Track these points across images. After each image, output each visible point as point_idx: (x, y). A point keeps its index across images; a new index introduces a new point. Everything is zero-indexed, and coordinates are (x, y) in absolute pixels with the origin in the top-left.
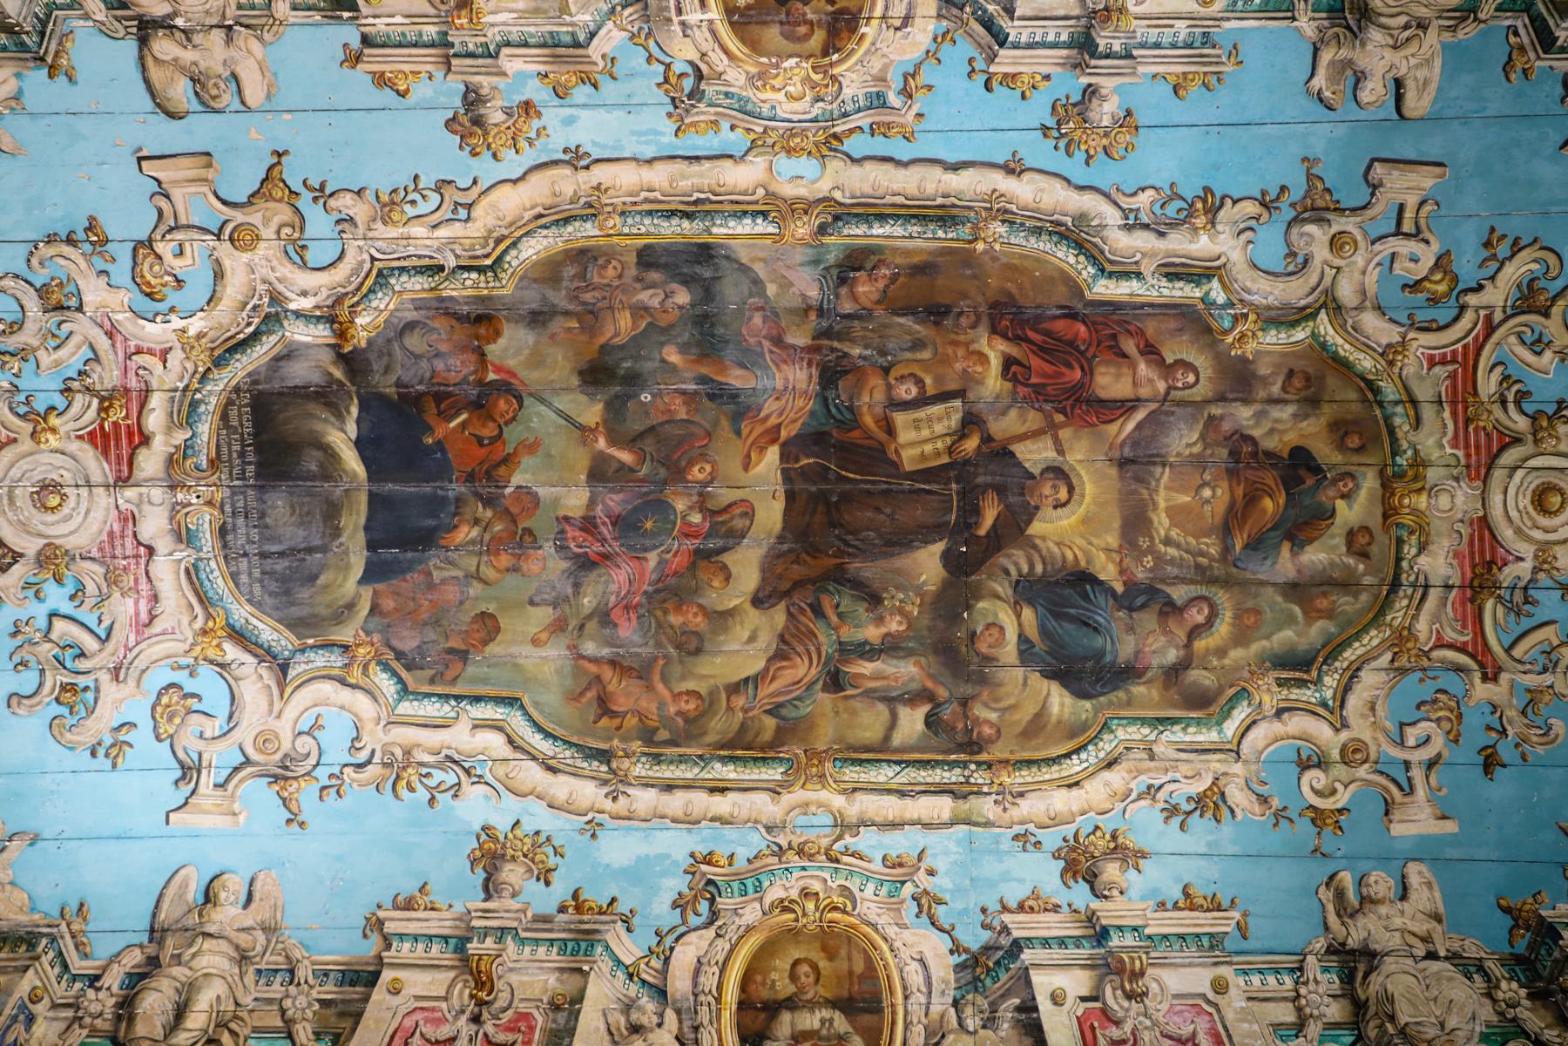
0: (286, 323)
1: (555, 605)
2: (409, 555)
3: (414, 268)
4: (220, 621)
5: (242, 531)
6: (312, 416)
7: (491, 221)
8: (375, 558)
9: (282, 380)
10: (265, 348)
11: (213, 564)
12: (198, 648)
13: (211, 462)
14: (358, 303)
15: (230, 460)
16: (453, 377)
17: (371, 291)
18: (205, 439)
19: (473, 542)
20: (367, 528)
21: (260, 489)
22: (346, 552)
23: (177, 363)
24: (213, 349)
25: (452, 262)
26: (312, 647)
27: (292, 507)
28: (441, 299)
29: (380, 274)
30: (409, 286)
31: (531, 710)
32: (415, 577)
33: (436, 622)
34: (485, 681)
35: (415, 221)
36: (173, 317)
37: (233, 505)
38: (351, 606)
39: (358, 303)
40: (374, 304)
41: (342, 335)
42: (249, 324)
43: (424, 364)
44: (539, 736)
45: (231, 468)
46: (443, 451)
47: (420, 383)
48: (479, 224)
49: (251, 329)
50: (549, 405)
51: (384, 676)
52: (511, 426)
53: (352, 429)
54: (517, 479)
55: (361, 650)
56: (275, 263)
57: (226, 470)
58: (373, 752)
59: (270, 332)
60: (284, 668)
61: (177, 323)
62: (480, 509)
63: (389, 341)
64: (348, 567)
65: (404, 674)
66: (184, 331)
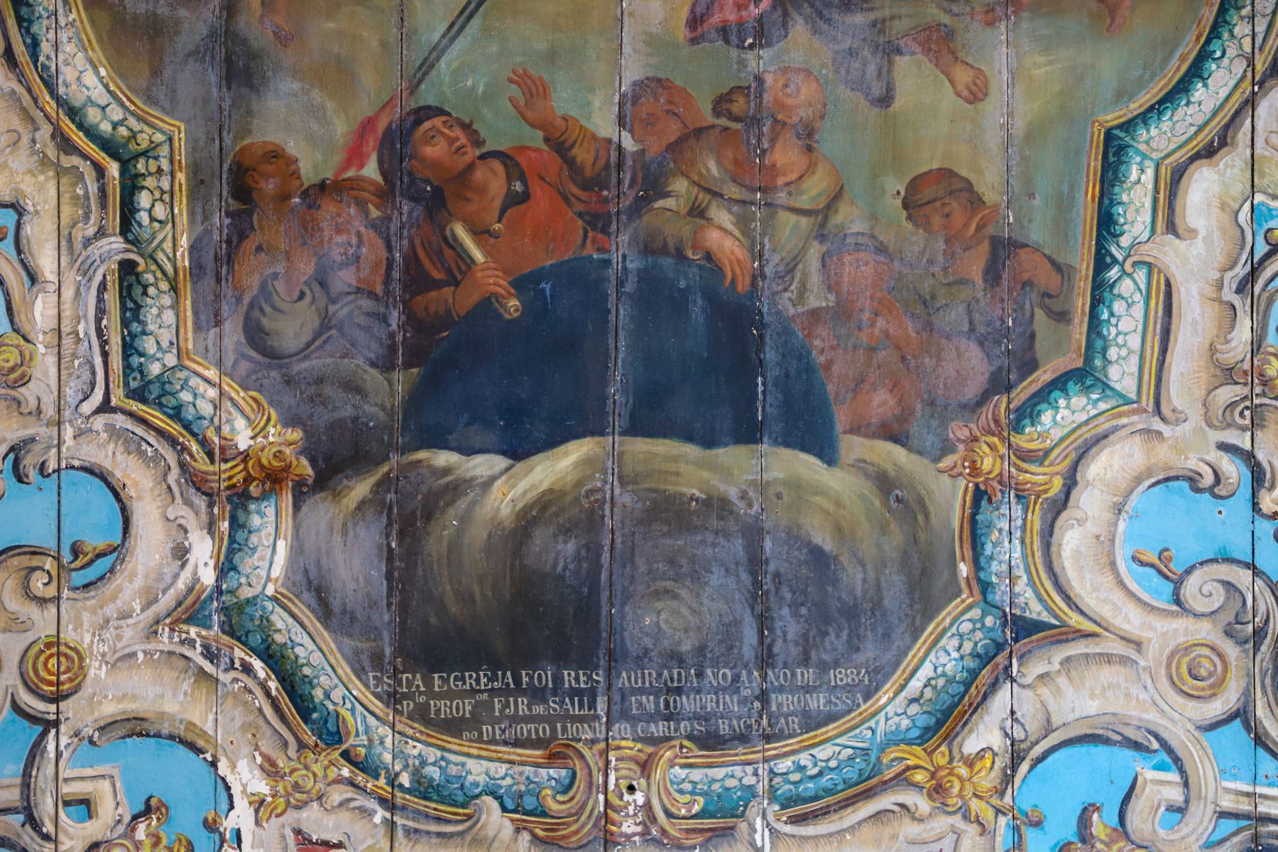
0: (246, 593)
1: (892, 50)
2: (770, 355)
3: (125, 323)
4: (915, 755)
5: (709, 702)
6: (454, 547)
7: (21, 161)
8: (778, 428)
9: (373, 604)
10: (301, 637)
11: (784, 765)
12: (975, 805)
13: (554, 758)
14: (204, 443)
15: (549, 720)
16: (373, 249)
17: (176, 414)
18: (503, 769)
19: (744, 222)
20: (709, 441)
21: (615, 659)
22: (762, 487)
23: (330, 821)
24: (302, 745)
25: (114, 245)
26: (977, 566)
27: (657, 595)
28: (197, 269)
29: (139, 395)
30: (166, 336)
31: (1135, 107)
32: (821, 345)
33: (927, 304)
34: (1064, 205)
35: (21, 319)
36: (229, 824)
37: (651, 718)
38: (885, 483)
39: (204, 443)
40: (206, 409)
41: (274, 479)
42: (247, 669)
43: (341, 311)
44: (1199, 92)
45: (567, 718)
46: (536, 277)
47: (384, 319)
48: (27, 185)
49: (258, 665)
50: (437, 51)
51: (1046, 417)
52: (483, 134)
53: (484, 465)
54: (603, 123)
55: (987, 464)
56: (110, 610)
57: (572, 729)
58: (1224, 447)
59: (266, 625)
60: (1024, 628)
61: (241, 817)
62: (669, 203)
63: (289, 381)
64: (796, 483)
65: (1044, 375)
66: (259, 804)
